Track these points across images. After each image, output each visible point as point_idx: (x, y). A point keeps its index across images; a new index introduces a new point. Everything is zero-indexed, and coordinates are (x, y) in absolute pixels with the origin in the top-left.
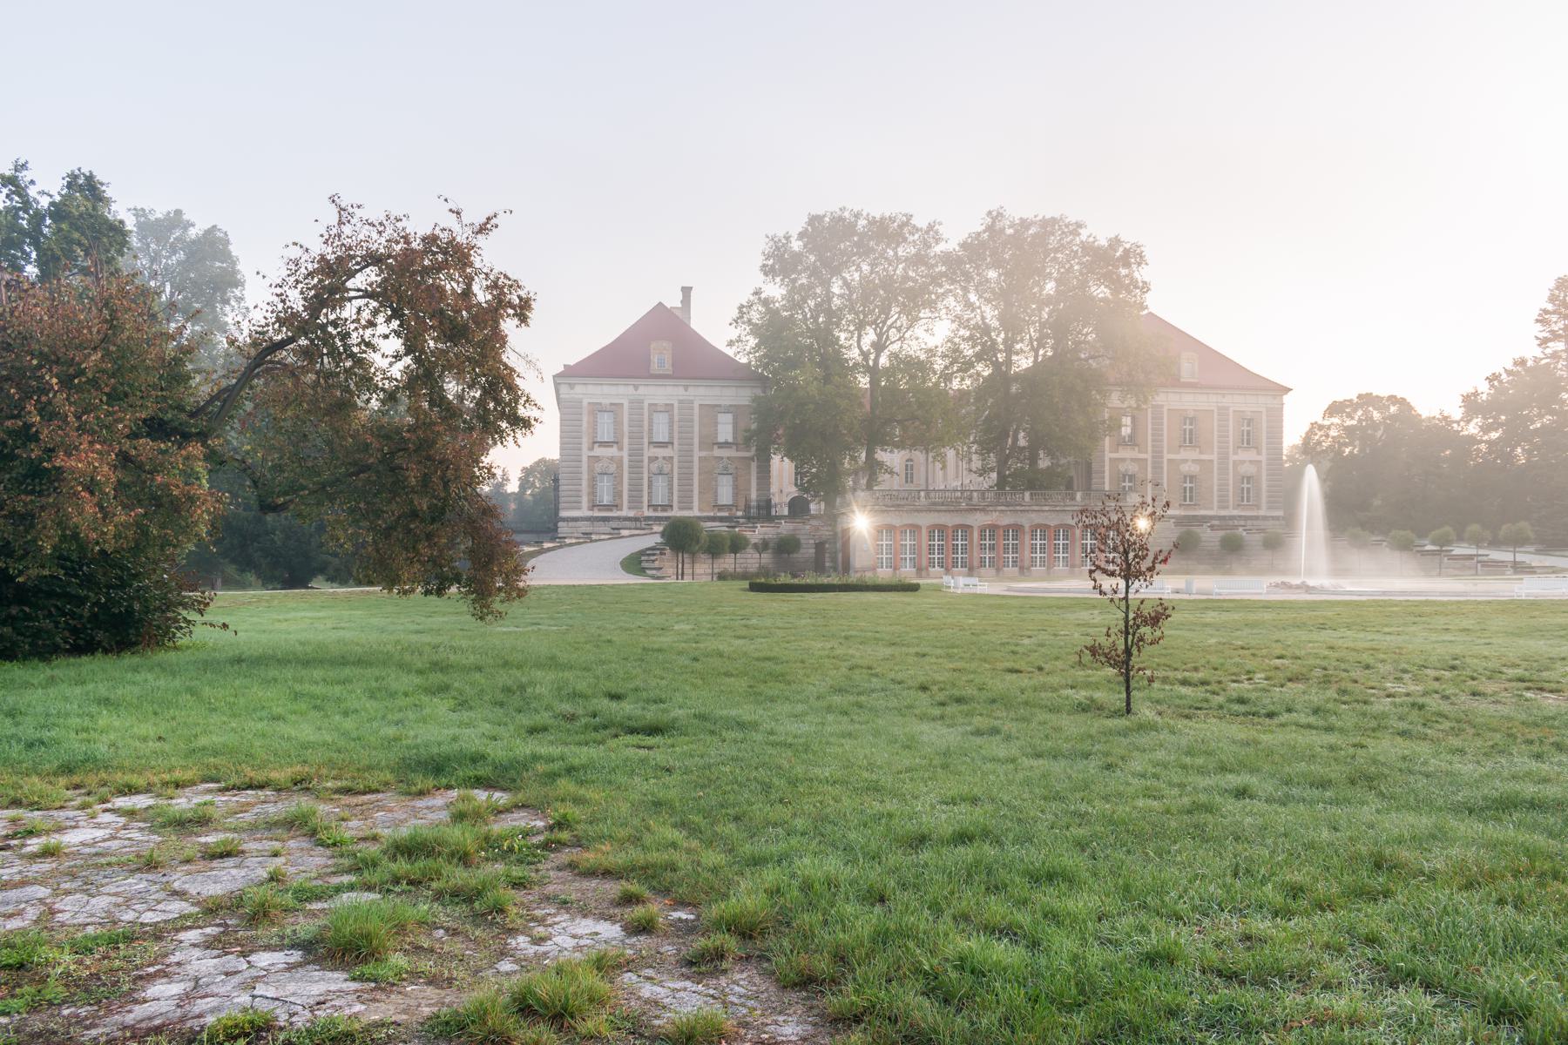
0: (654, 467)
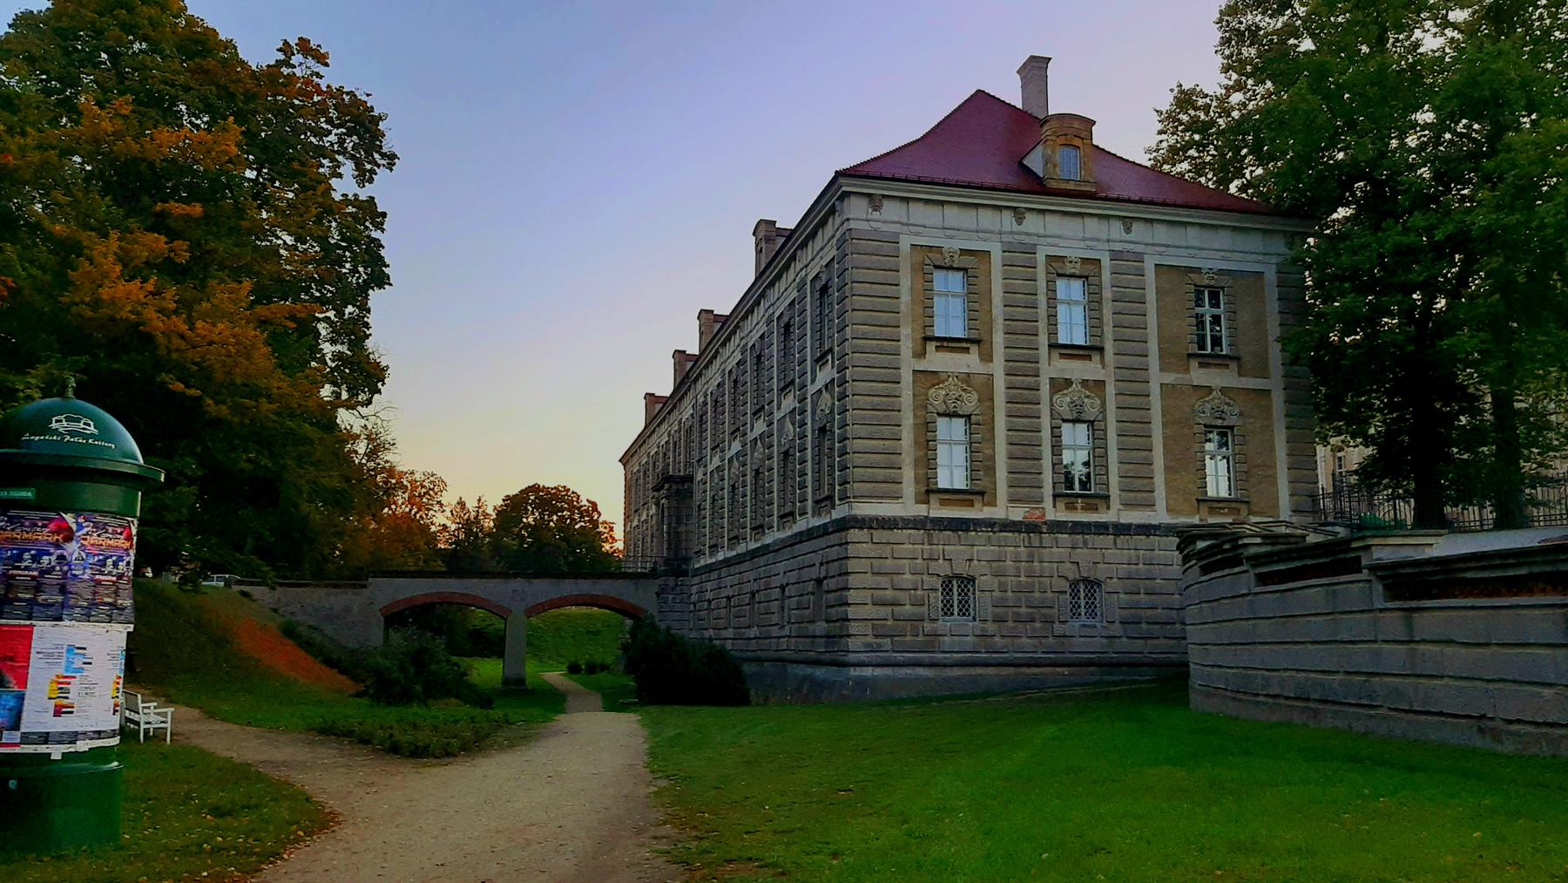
0: (1064, 402)
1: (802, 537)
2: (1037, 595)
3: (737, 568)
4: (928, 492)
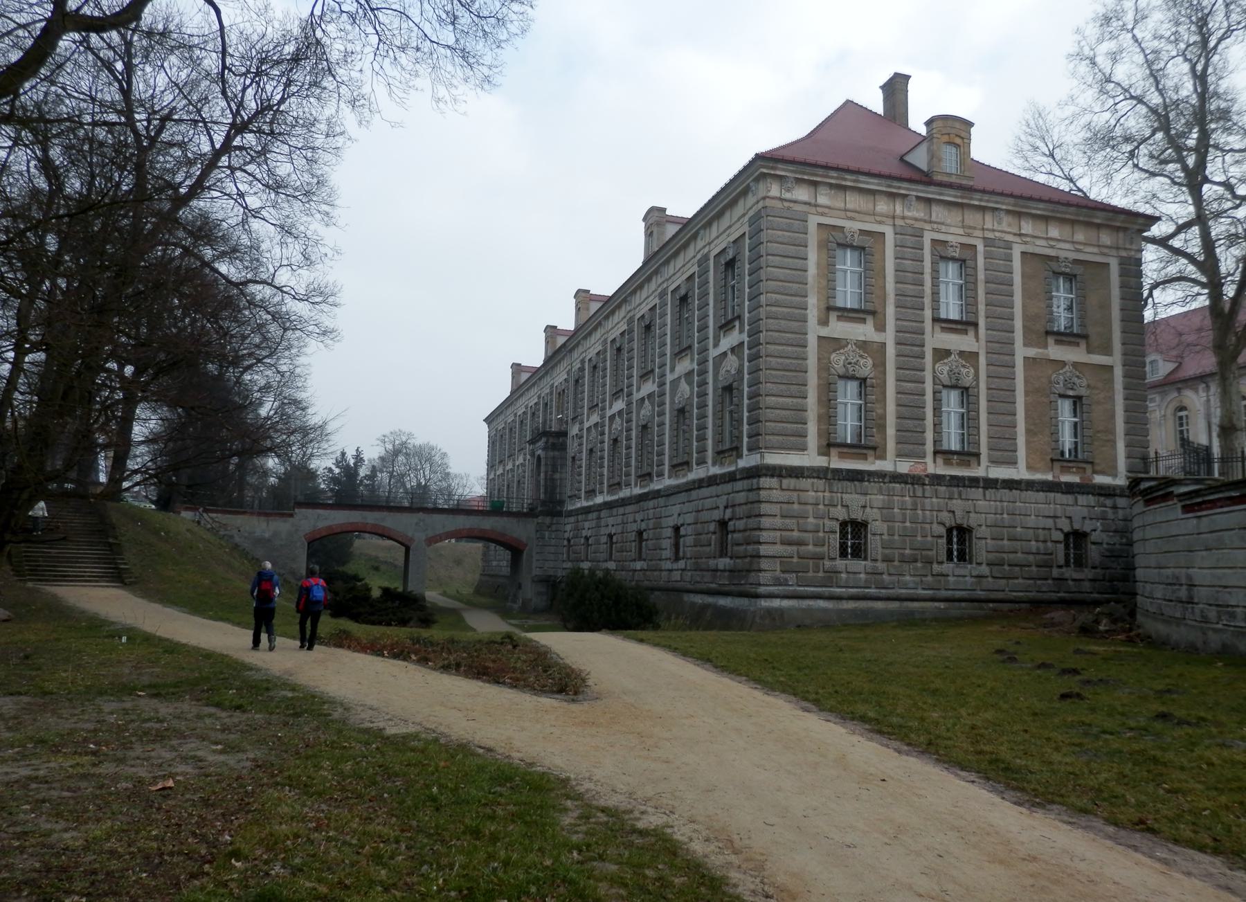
1: (700, 484)
2: (919, 538)
3: (621, 510)
4: (829, 445)
